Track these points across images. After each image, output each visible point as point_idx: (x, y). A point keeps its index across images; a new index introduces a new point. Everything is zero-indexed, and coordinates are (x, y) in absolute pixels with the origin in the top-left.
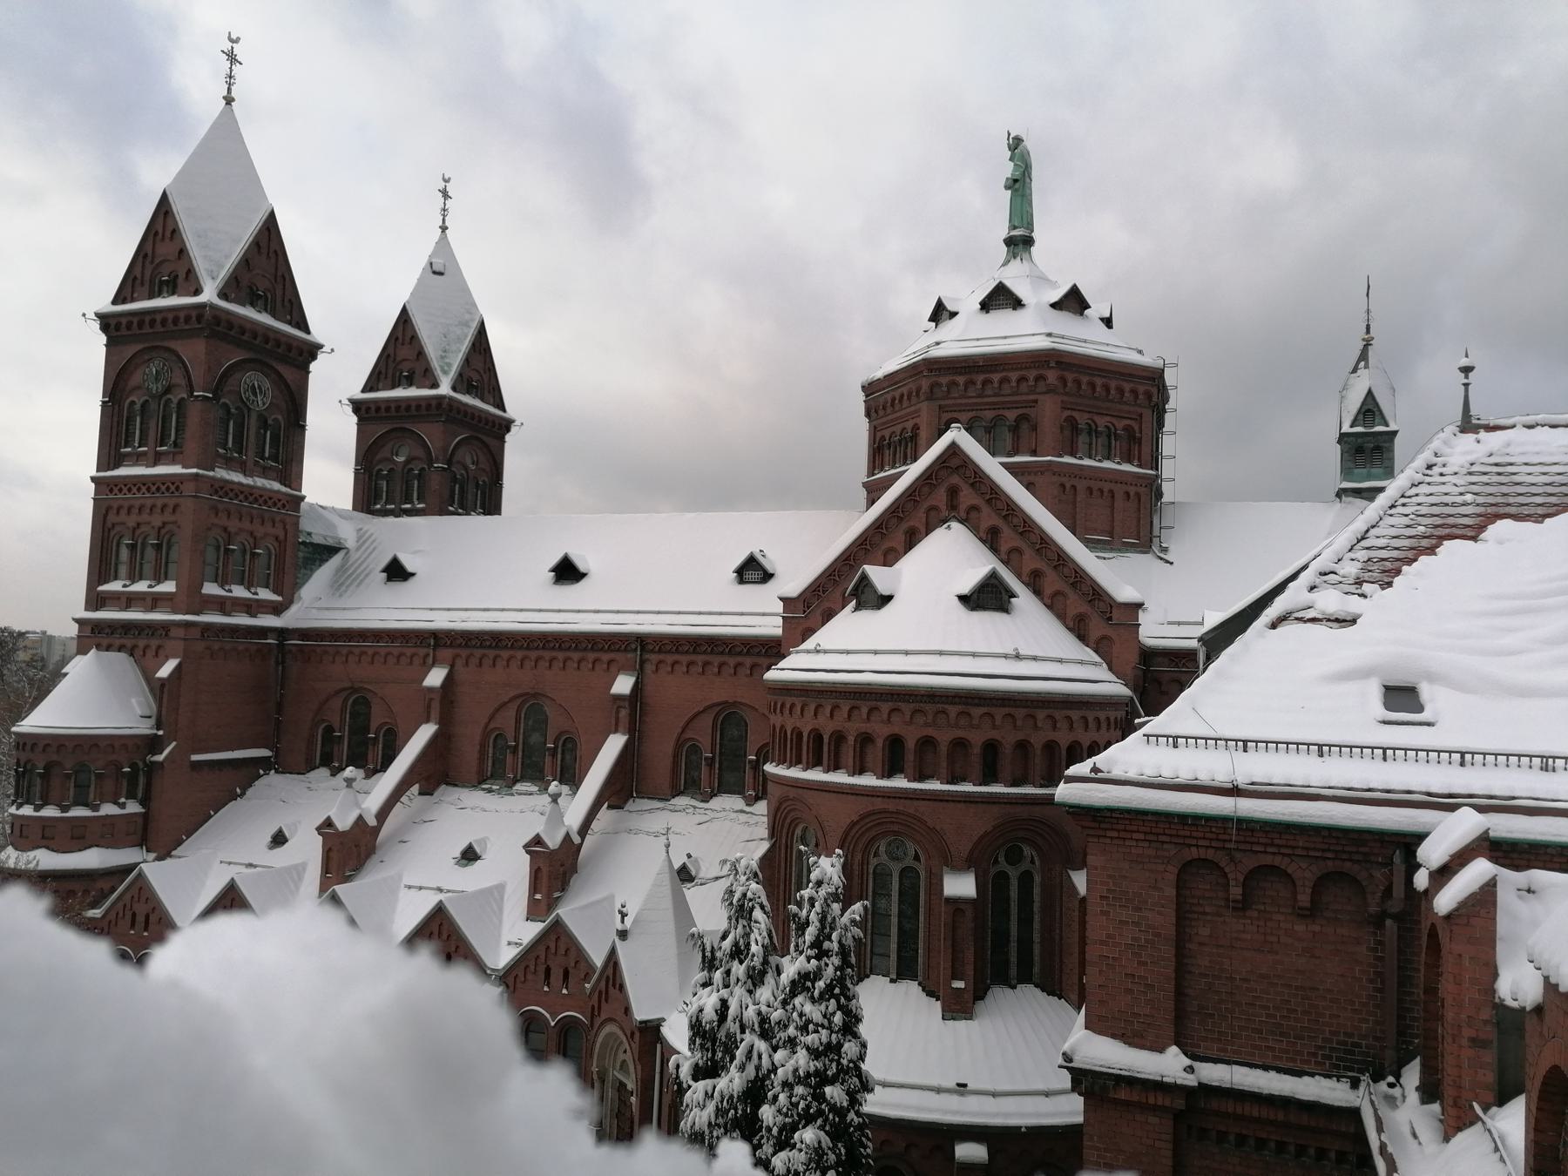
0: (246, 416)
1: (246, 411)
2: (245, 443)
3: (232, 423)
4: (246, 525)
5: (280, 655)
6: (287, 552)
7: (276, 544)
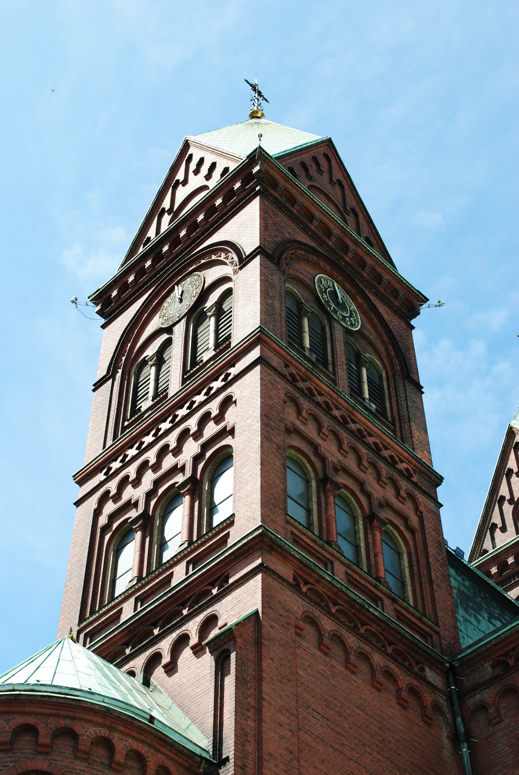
0: (327, 328)
1: (326, 322)
2: (330, 358)
3: (306, 321)
4: (351, 463)
5: (459, 719)
6: (430, 549)
7: (408, 536)
